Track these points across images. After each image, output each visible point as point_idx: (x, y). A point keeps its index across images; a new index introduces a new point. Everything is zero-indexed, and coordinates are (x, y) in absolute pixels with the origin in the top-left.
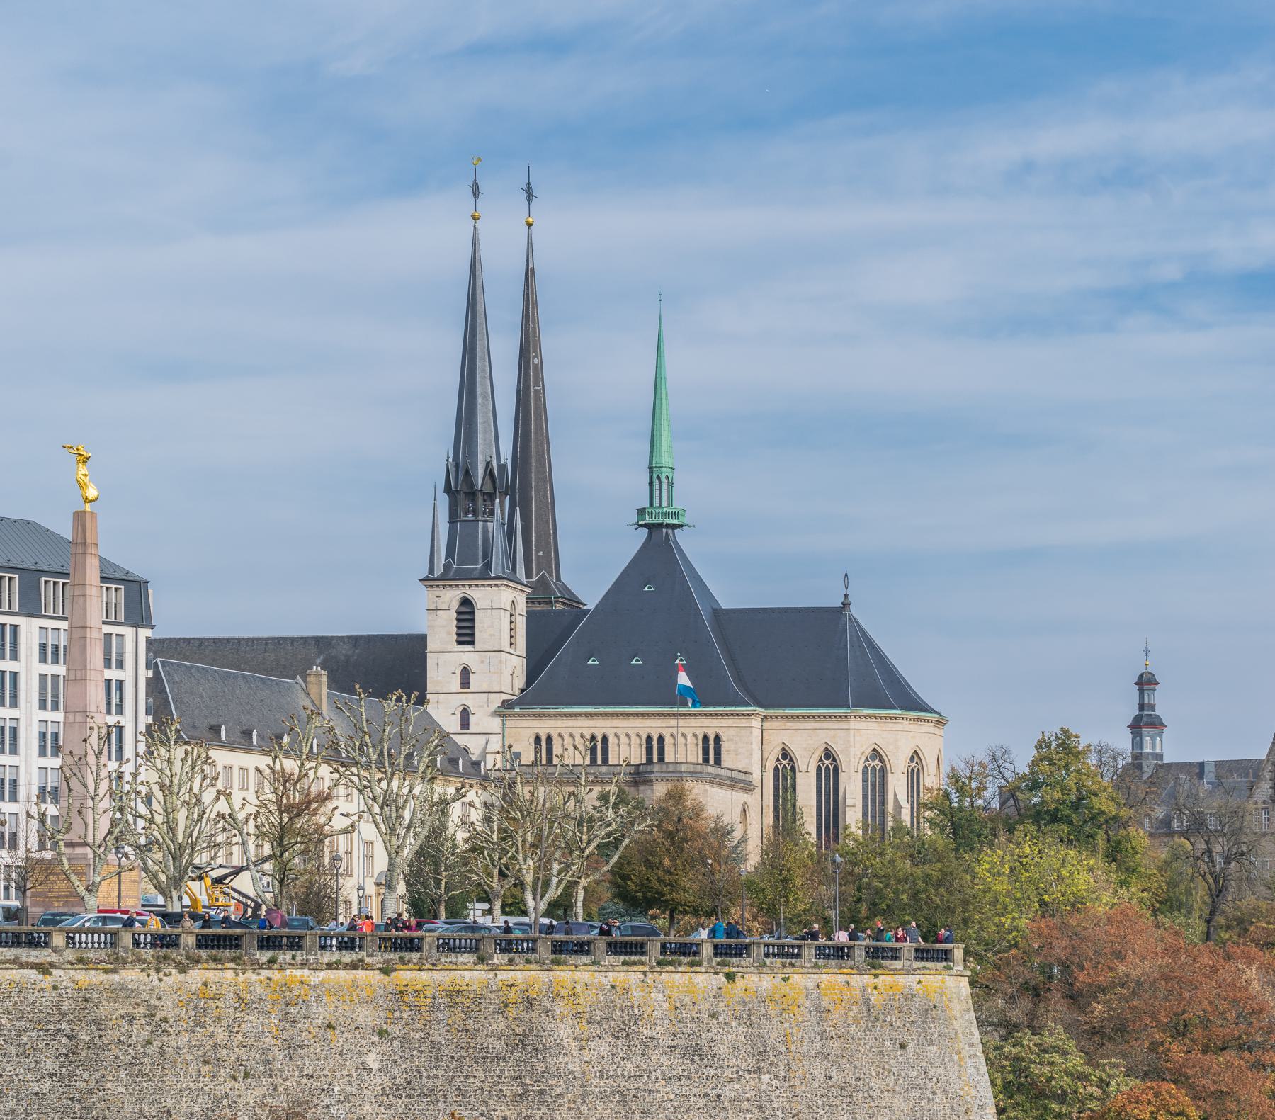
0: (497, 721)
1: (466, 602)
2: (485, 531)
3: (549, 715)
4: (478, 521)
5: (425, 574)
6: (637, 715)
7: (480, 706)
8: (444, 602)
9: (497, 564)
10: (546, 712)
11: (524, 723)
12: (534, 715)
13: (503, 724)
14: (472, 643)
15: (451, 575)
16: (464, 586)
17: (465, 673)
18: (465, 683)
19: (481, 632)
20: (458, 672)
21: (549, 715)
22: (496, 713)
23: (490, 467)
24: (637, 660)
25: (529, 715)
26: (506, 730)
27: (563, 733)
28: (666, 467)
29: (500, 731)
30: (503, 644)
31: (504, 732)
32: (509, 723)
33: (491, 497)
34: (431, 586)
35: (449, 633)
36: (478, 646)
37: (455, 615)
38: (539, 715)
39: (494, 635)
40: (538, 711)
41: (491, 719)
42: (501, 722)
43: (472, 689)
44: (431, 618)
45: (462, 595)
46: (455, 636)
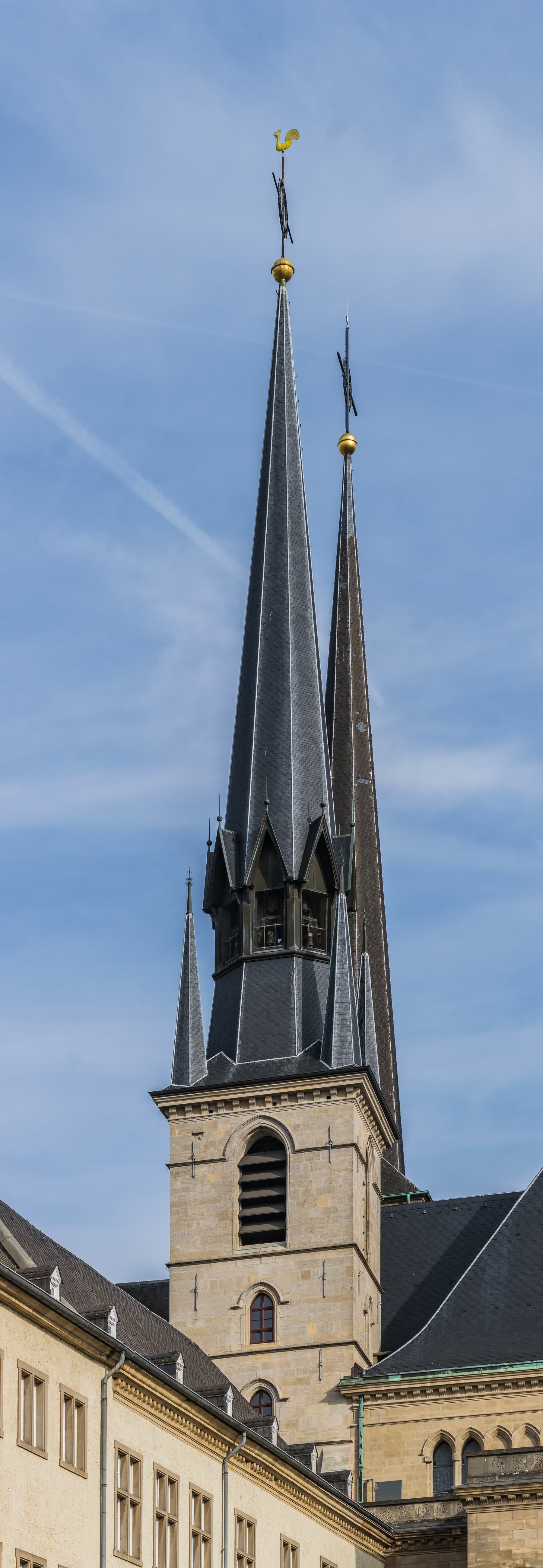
0: (343, 1412)
2: (309, 982)
4: (291, 955)
5: (166, 1081)
8: (212, 1144)
9: (343, 1042)
11: (409, 1411)
13: (358, 1417)
14: (280, 1236)
15: (229, 1078)
16: (261, 1100)
19: (301, 1205)
21: (475, 1387)
23: (321, 829)
25: (423, 1391)
27: (509, 1426)
29: (350, 1435)
30: (355, 1233)
31: (358, 1435)
34: (181, 1109)
37: (237, 1173)
38: (449, 1389)
39: (336, 1210)
40: (447, 1376)
41: (326, 1407)
42: (351, 1415)
43: (279, 1343)
44: (178, 1184)
45: (256, 1124)
46: (237, 1225)
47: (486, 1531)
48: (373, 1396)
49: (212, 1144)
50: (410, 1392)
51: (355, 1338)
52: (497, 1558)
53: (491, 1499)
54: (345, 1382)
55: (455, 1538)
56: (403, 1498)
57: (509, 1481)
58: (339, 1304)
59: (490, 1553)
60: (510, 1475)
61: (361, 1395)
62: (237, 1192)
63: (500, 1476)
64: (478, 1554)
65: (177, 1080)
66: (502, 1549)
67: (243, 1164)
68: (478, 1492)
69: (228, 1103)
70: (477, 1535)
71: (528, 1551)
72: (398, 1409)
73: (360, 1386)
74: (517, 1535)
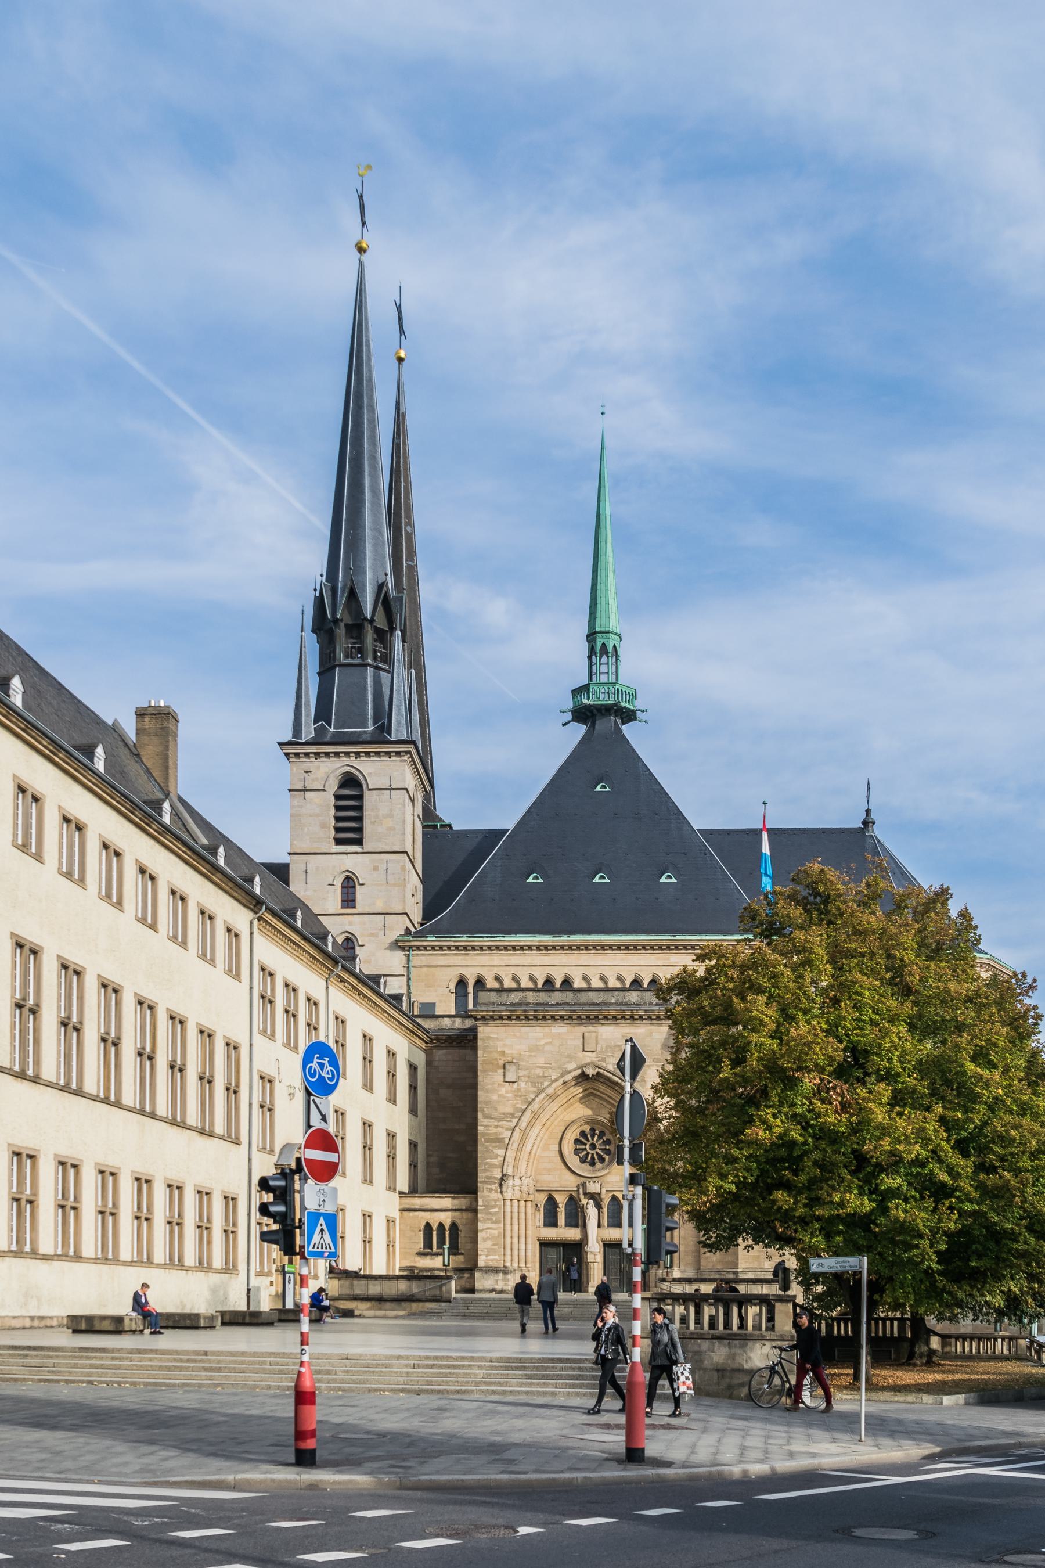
0: (399, 956)
1: (350, 782)
3: (481, 948)
6: (619, 948)
7: (372, 935)
10: (477, 941)
11: (440, 959)
12: (457, 948)
13: (409, 961)
17: (349, 885)
18: (349, 900)
19: (373, 823)
20: (338, 883)
22: (396, 945)
24: (602, 877)
25: (449, 948)
26: (412, 970)
28: (614, 633)
29: (403, 971)
31: (409, 972)
32: (418, 959)
33: (383, 637)
35: (323, 826)
36: (368, 846)
41: (388, 952)
42: (404, 959)
47: (489, 1038)
48: (418, 948)
49: (317, 779)
50: (441, 948)
51: (406, 911)
52: (496, 1055)
53: (492, 1018)
54: (401, 938)
55: (470, 1041)
56: (437, 1013)
57: (503, 1008)
58: (396, 888)
59: (491, 1052)
60: (504, 1004)
61: (410, 947)
62: (333, 811)
63: (498, 1004)
64: (484, 1051)
65: (294, 736)
66: (499, 1050)
67: (337, 794)
68: (484, 1013)
69: (327, 755)
70: (483, 1039)
71: (515, 1052)
72: (433, 957)
73: (410, 941)
74: (508, 1042)
